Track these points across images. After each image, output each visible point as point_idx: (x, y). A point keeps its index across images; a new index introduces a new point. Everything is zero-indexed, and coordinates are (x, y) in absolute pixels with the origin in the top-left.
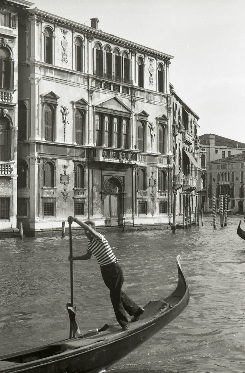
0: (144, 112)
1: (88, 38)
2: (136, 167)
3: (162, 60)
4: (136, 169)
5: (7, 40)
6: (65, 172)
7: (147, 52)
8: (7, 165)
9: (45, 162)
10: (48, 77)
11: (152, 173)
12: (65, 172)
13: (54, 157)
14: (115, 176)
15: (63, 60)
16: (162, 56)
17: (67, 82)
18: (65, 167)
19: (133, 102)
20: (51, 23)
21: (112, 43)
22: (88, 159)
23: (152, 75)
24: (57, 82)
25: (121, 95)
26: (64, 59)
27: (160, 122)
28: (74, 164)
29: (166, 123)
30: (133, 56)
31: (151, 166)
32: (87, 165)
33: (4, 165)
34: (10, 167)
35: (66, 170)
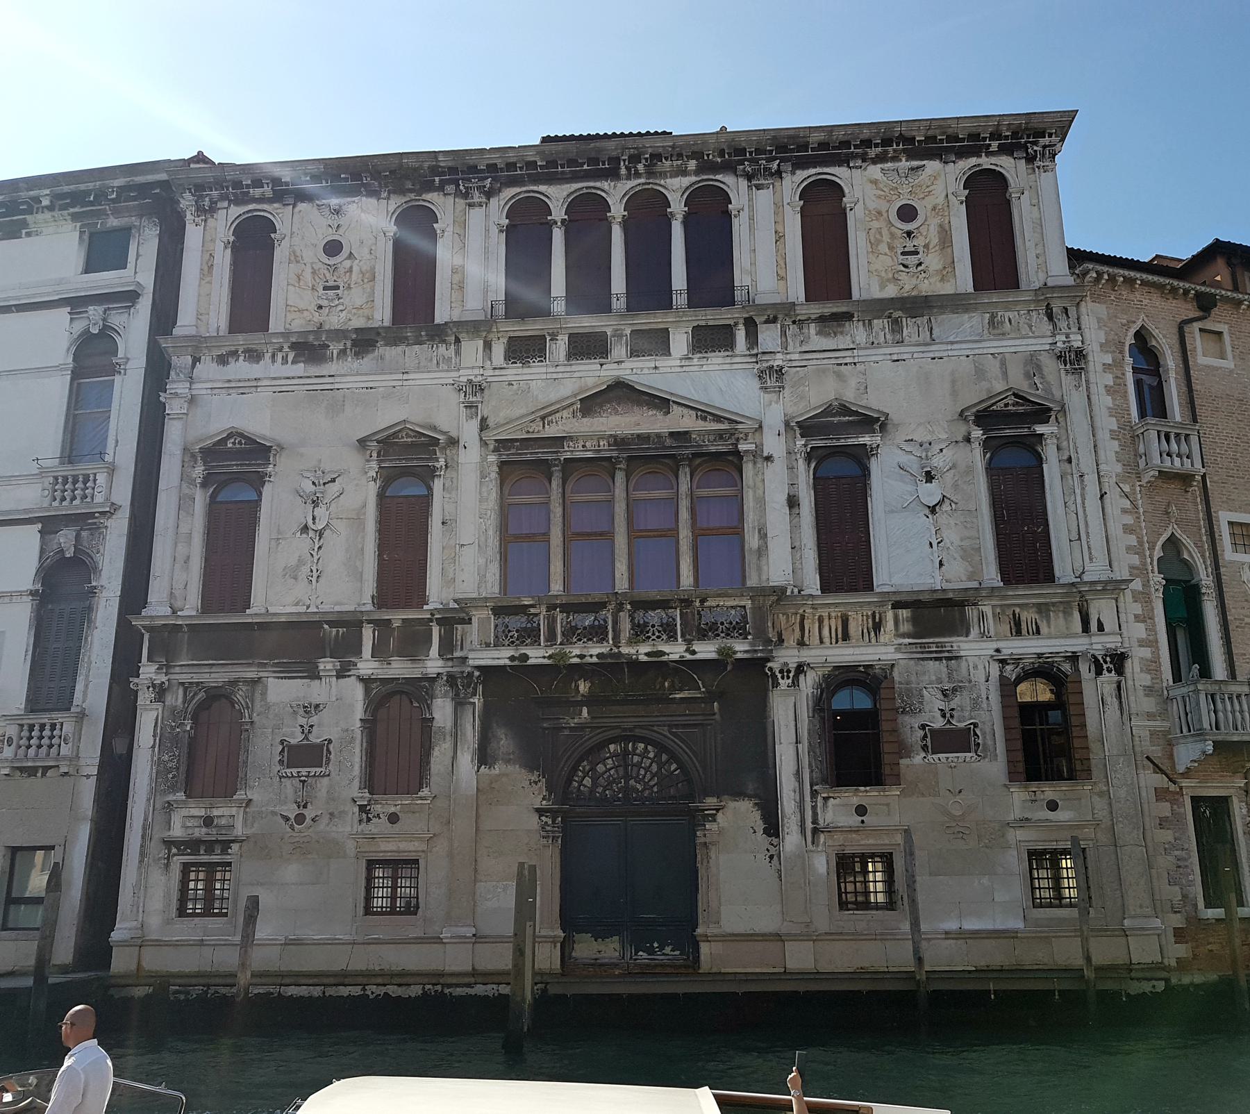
0: (844, 409)
1: (458, 194)
2: (796, 676)
3: (989, 154)
4: (795, 683)
5: (95, 311)
6: (307, 731)
7: (856, 147)
8: (53, 727)
9: (193, 697)
10: (233, 385)
11: (945, 693)
12: (307, 731)
13: (251, 673)
14: (641, 727)
15: (320, 307)
16: (974, 136)
17: (338, 379)
18: (312, 709)
19: (772, 377)
20: (261, 200)
21: (613, 174)
22: (450, 664)
23: (909, 234)
24: (284, 389)
25: (678, 363)
26: (324, 303)
27: (993, 434)
28: (367, 691)
29: (1040, 429)
30: (758, 187)
31: (936, 659)
32: (441, 688)
33: (42, 727)
34: (61, 730)
35: (314, 720)
